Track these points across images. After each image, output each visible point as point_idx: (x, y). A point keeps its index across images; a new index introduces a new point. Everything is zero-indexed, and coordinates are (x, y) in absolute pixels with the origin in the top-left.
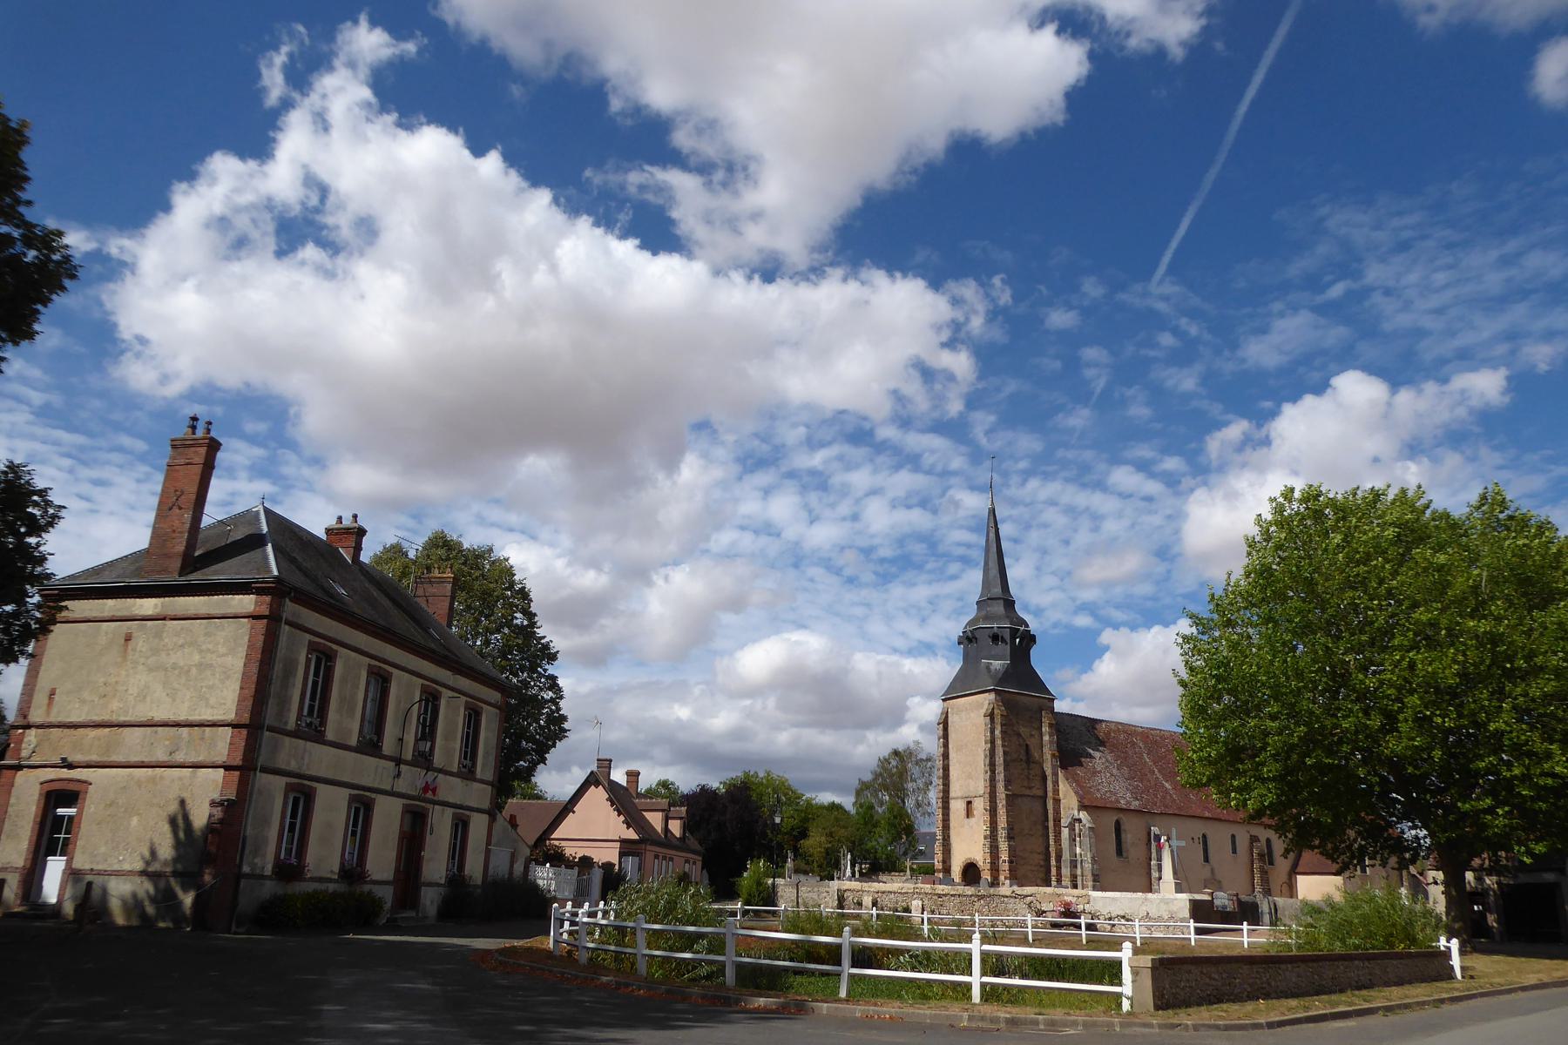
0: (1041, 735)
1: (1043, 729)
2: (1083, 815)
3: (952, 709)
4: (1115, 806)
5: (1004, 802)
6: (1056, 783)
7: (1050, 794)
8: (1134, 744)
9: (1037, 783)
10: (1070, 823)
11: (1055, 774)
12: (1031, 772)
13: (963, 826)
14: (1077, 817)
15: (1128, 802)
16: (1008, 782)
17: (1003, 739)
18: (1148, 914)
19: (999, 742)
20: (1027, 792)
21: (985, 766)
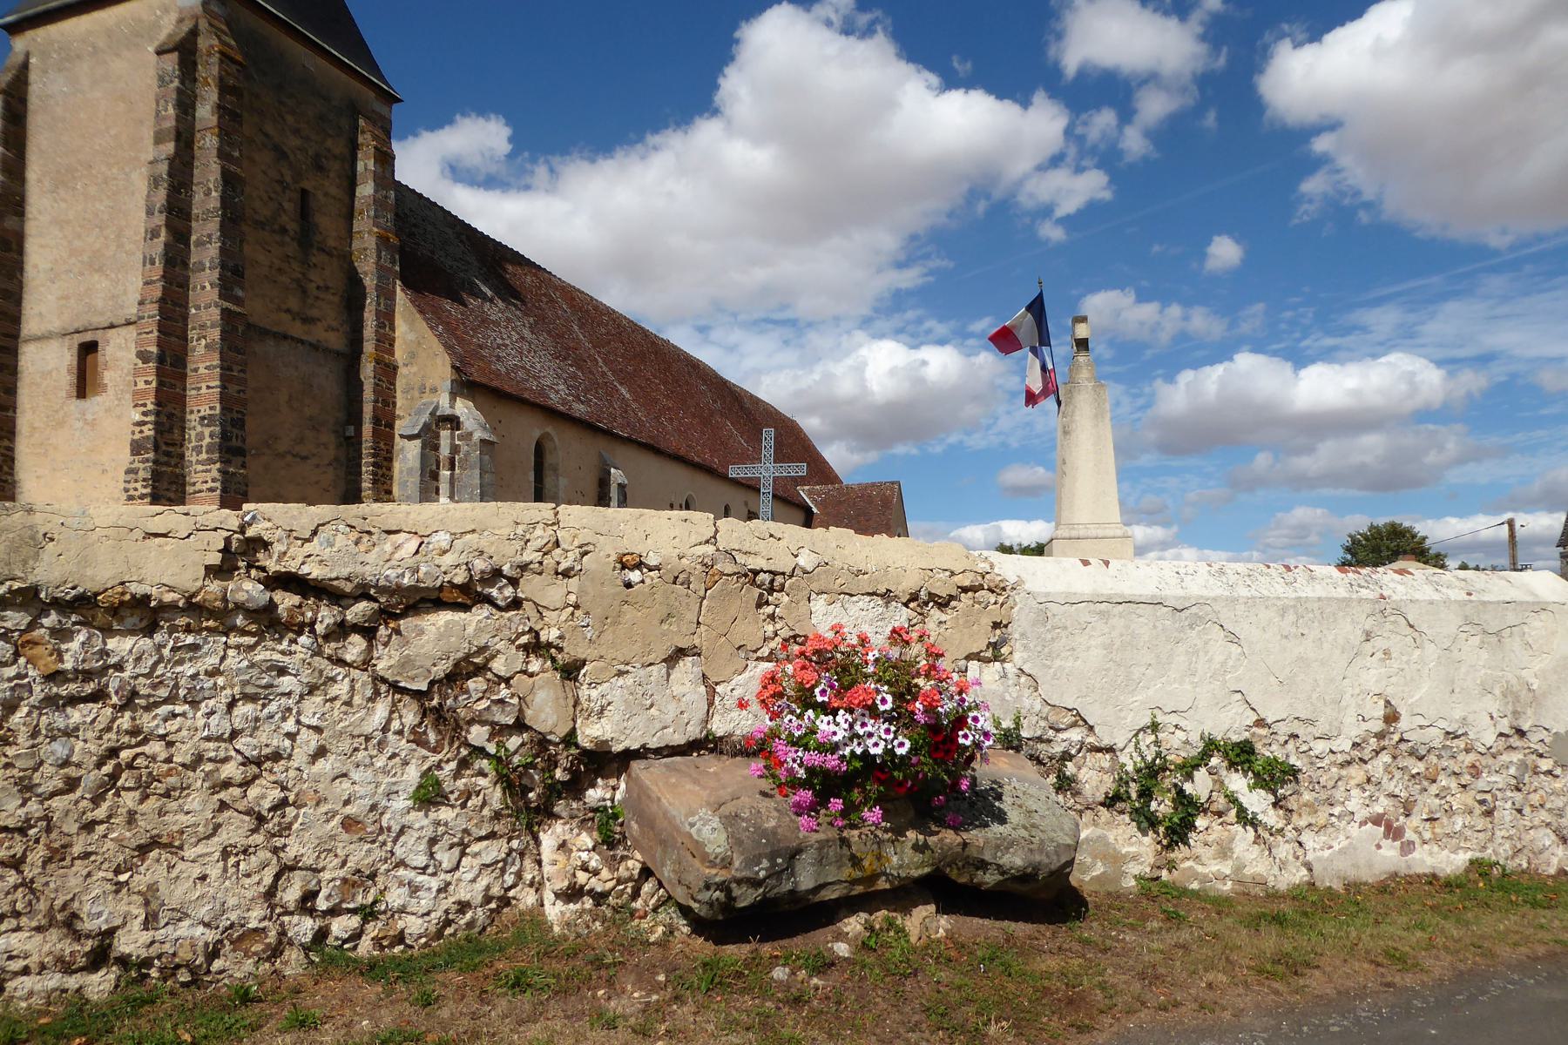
0: (352, 183)
1: (360, 166)
2: (464, 409)
3: (45, 55)
4: (540, 400)
5: (215, 334)
6: (386, 318)
7: (369, 347)
8: (552, 301)
9: (329, 311)
10: (426, 427)
11: (387, 295)
12: (313, 275)
13: (61, 424)
14: (448, 412)
15: (564, 402)
16: (232, 275)
17: (224, 132)
18: (1392, 717)
19: (208, 143)
20: (297, 329)
21: (150, 212)
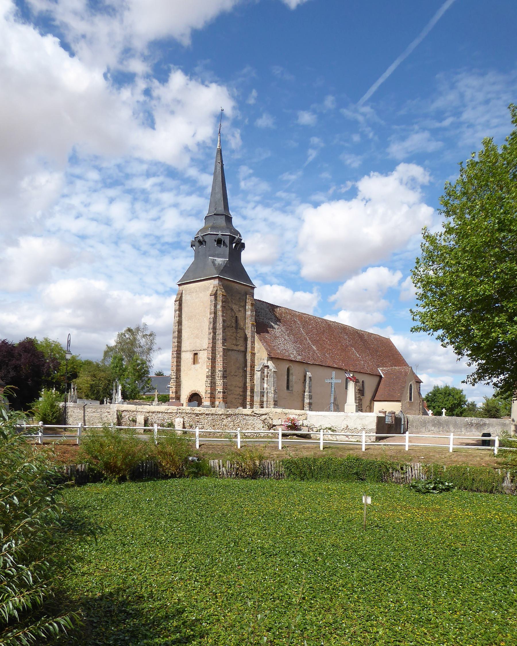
1: (247, 307)
2: (270, 364)
3: (186, 291)
5: (222, 353)
6: (253, 342)
7: (249, 349)
8: (295, 322)
9: (241, 342)
10: (262, 368)
11: (253, 337)
13: (190, 370)
15: (295, 357)
16: (224, 340)
18: (347, 426)
19: (220, 313)
20: (235, 348)
21: (209, 329)
